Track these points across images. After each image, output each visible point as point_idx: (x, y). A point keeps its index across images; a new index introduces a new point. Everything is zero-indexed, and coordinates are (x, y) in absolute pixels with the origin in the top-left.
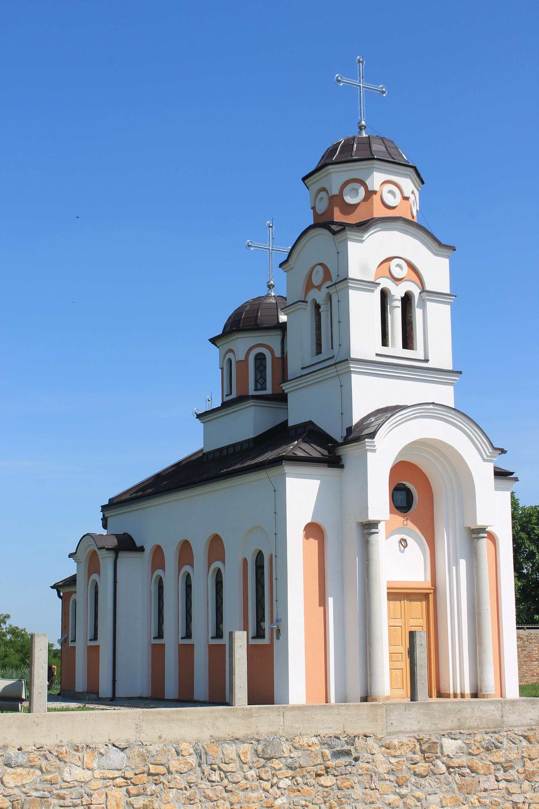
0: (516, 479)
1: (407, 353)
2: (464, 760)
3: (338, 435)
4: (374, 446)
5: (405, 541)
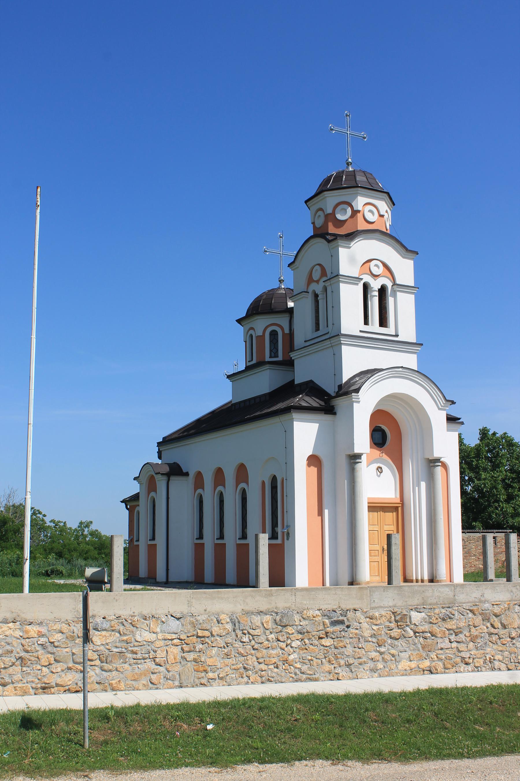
0: (462, 423)
1: (383, 330)
2: (426, 627)
3: (331, 390)
4: (359, 398)
5: (381, 468)
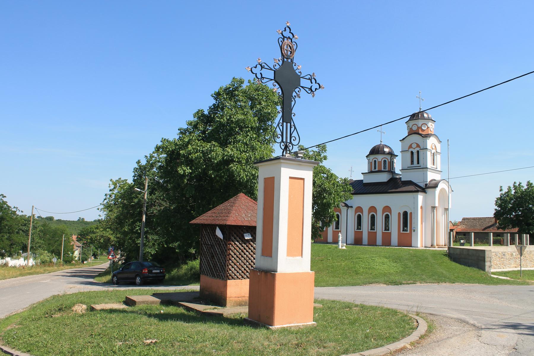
3: (422, 185)
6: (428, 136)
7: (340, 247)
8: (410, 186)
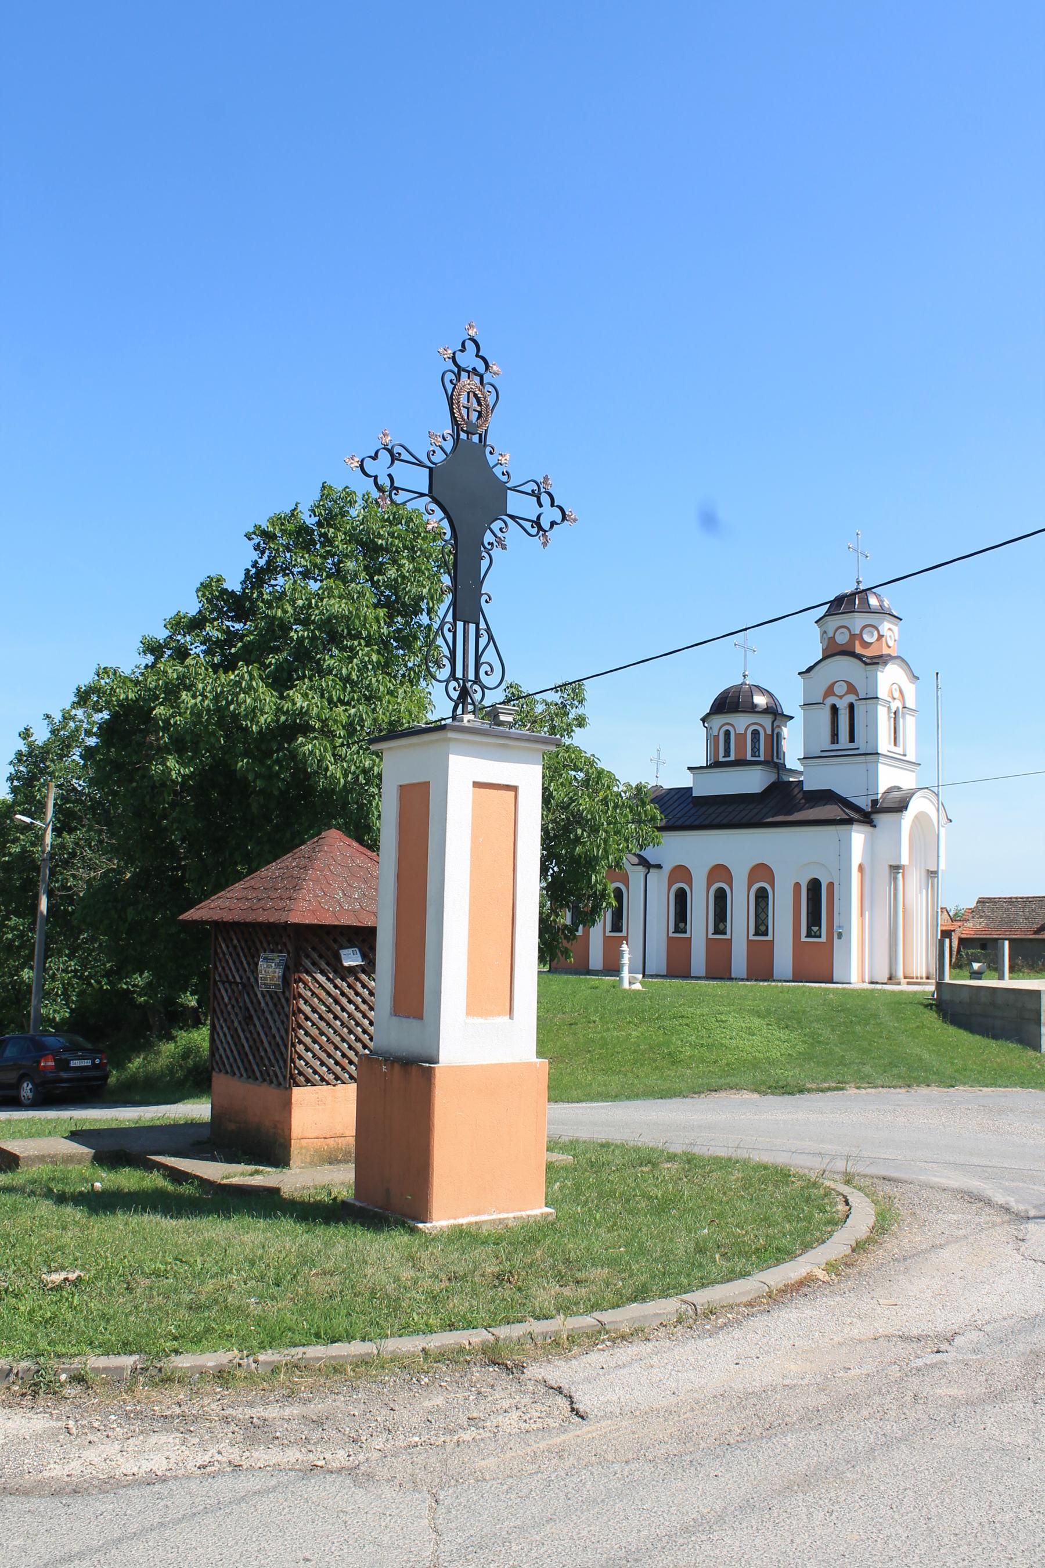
3: (864, 803)
6: (879, 661)
7: (626, 985)
8: (829, 807)
